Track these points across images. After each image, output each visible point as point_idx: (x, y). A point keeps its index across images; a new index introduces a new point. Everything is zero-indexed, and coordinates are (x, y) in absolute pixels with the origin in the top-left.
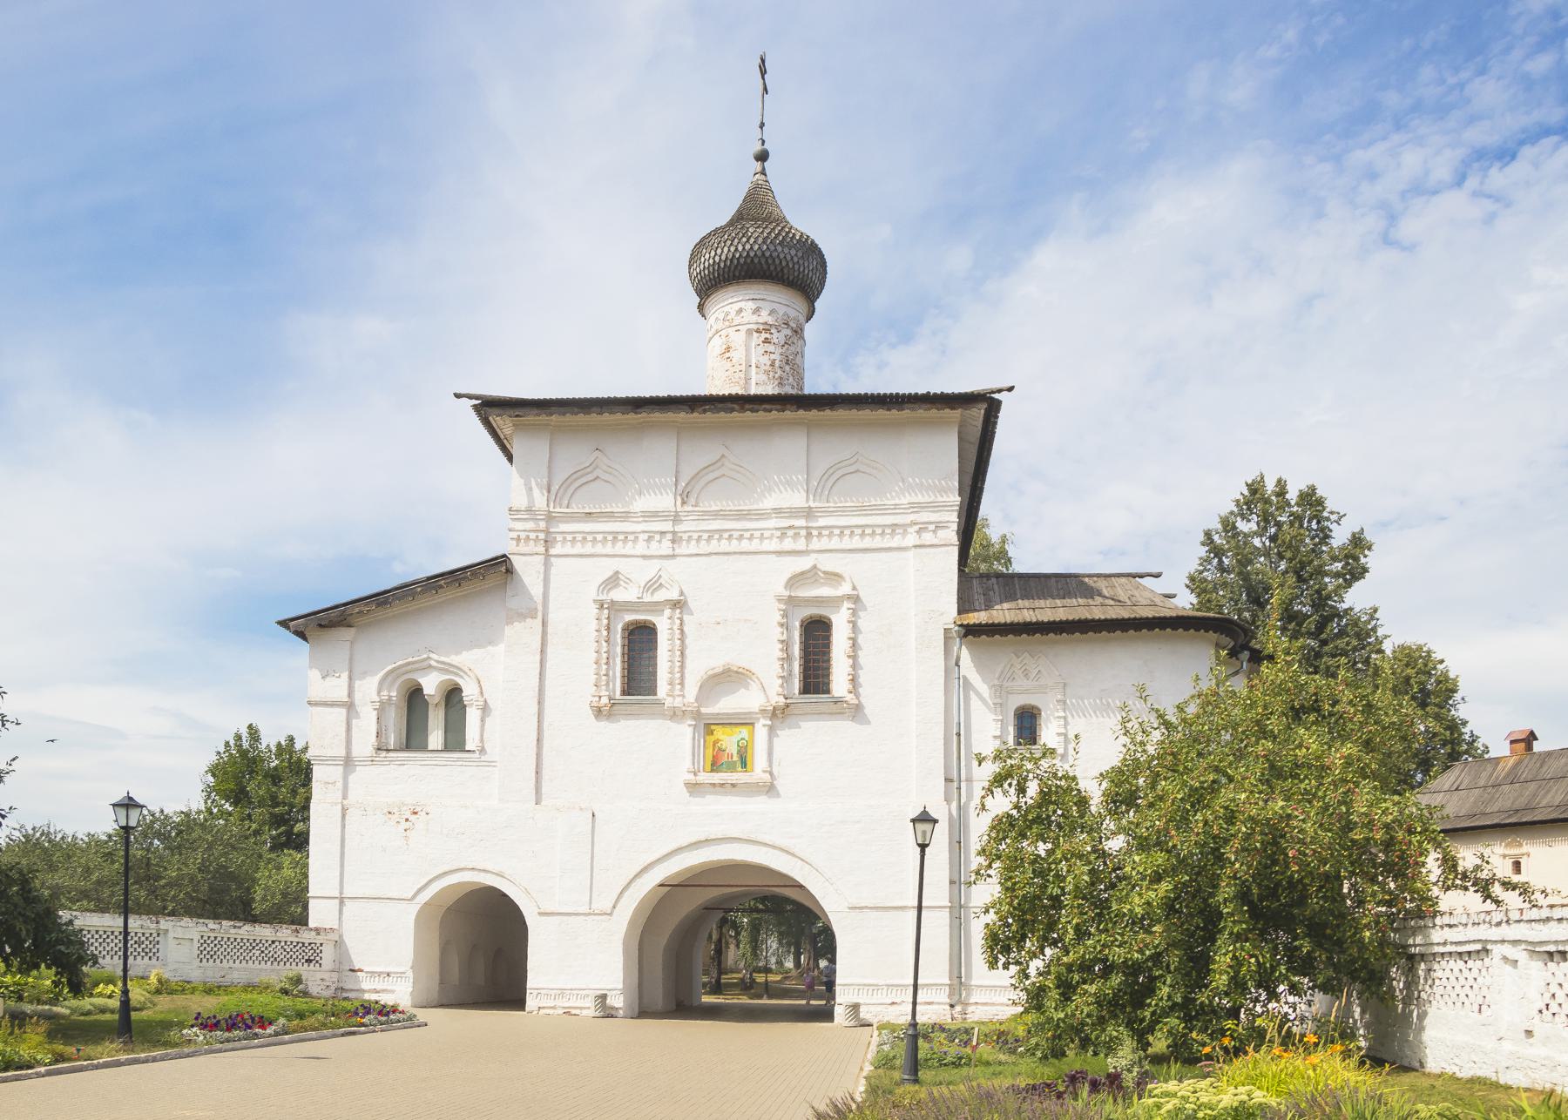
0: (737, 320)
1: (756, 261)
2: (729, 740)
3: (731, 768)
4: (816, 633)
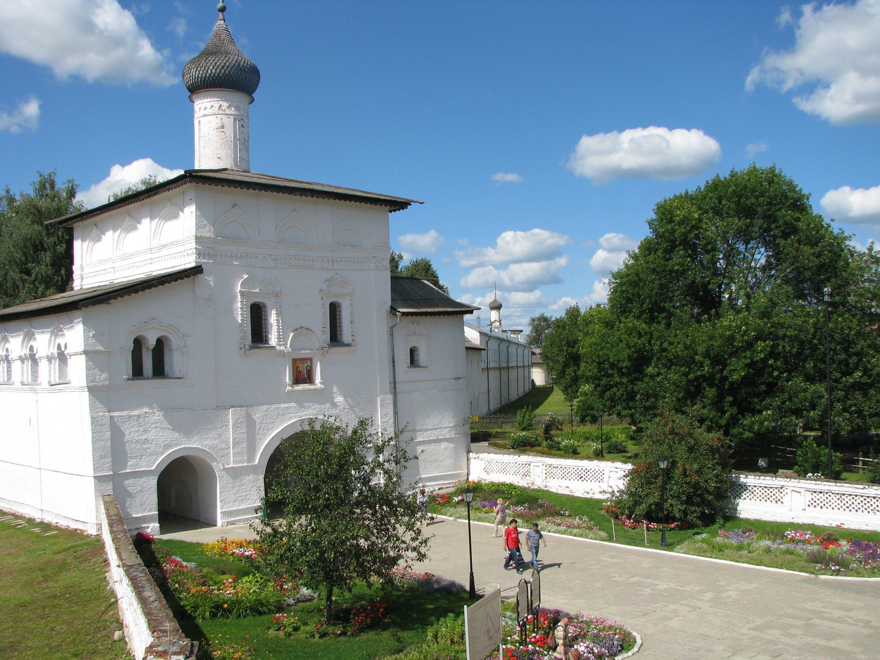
0: (228, 112)
1: (242, 81)
2: (303, 368)
3: (304, 381)
4: (334, 310)
